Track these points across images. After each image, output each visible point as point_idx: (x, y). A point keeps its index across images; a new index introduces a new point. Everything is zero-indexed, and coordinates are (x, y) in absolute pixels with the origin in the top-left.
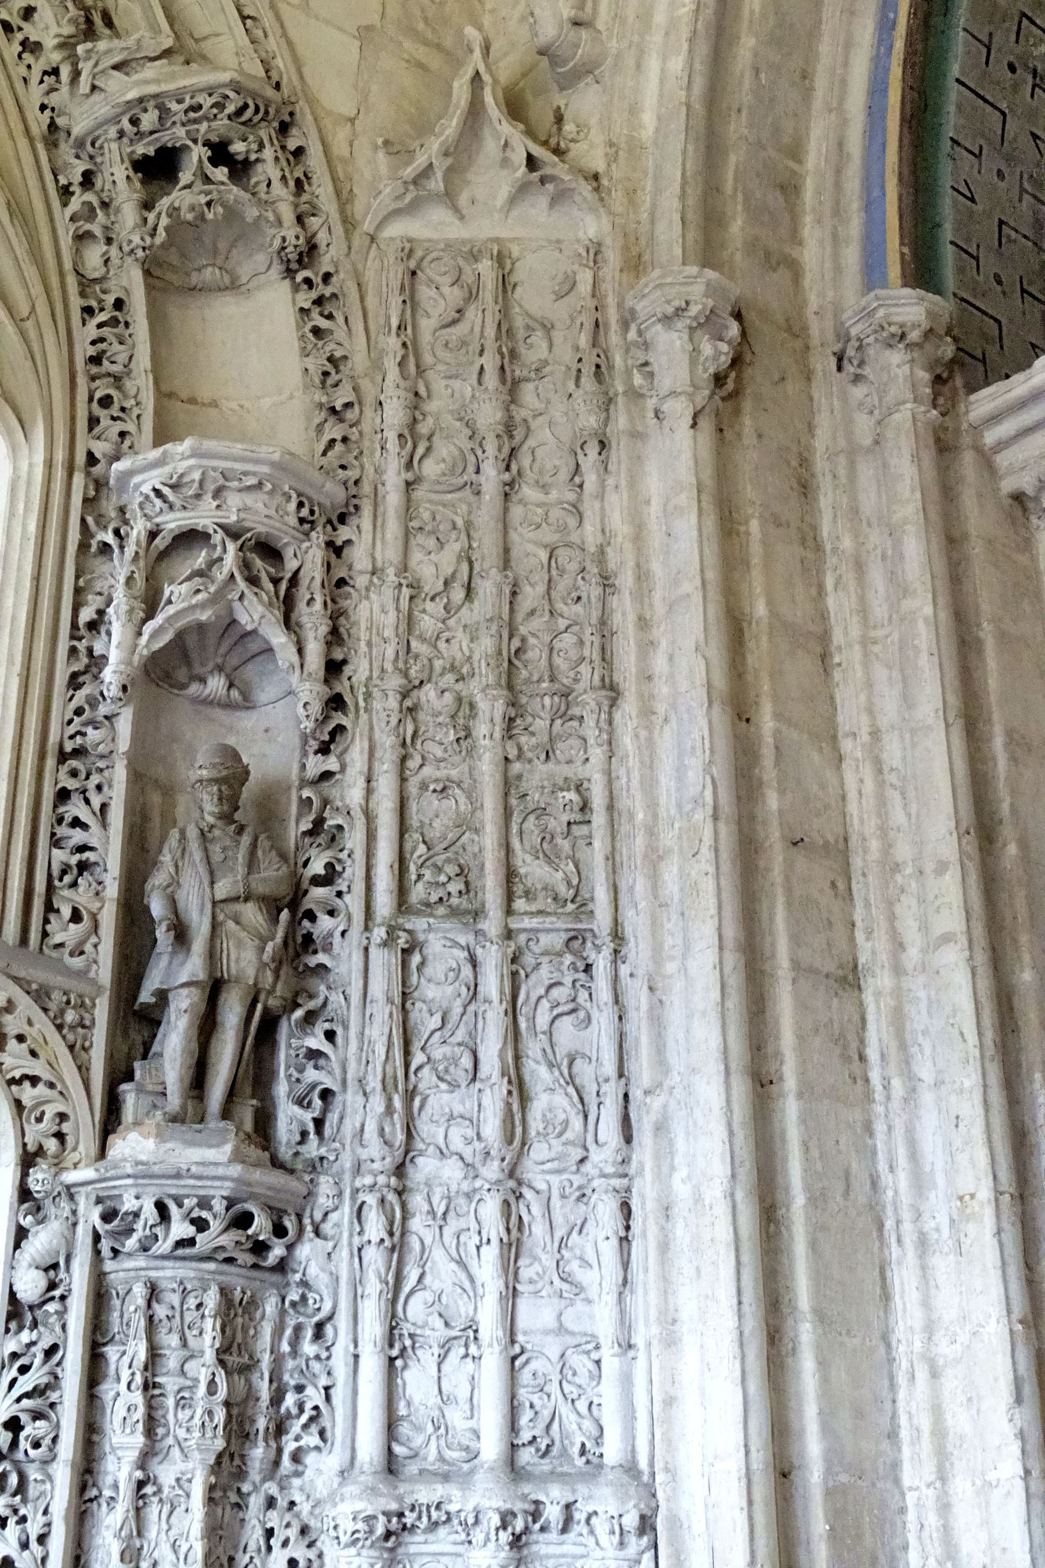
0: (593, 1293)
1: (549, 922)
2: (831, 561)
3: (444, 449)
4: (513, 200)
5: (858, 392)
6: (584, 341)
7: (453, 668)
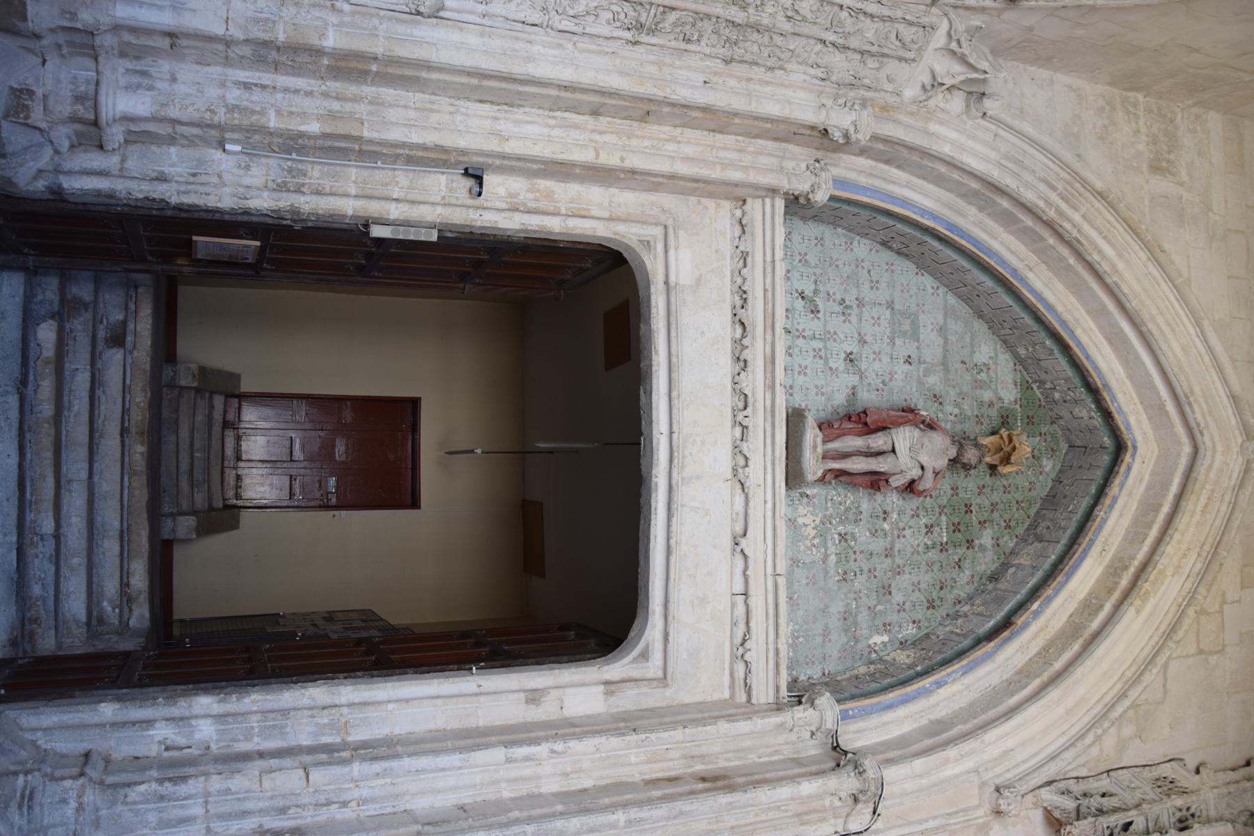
0: (507, 5)
1: (650, 19)
2: (748, 140)
3: (849, 21)
4: (933, 72)
5: (803, 166)
6: (866, 81)
7: (762, 4)
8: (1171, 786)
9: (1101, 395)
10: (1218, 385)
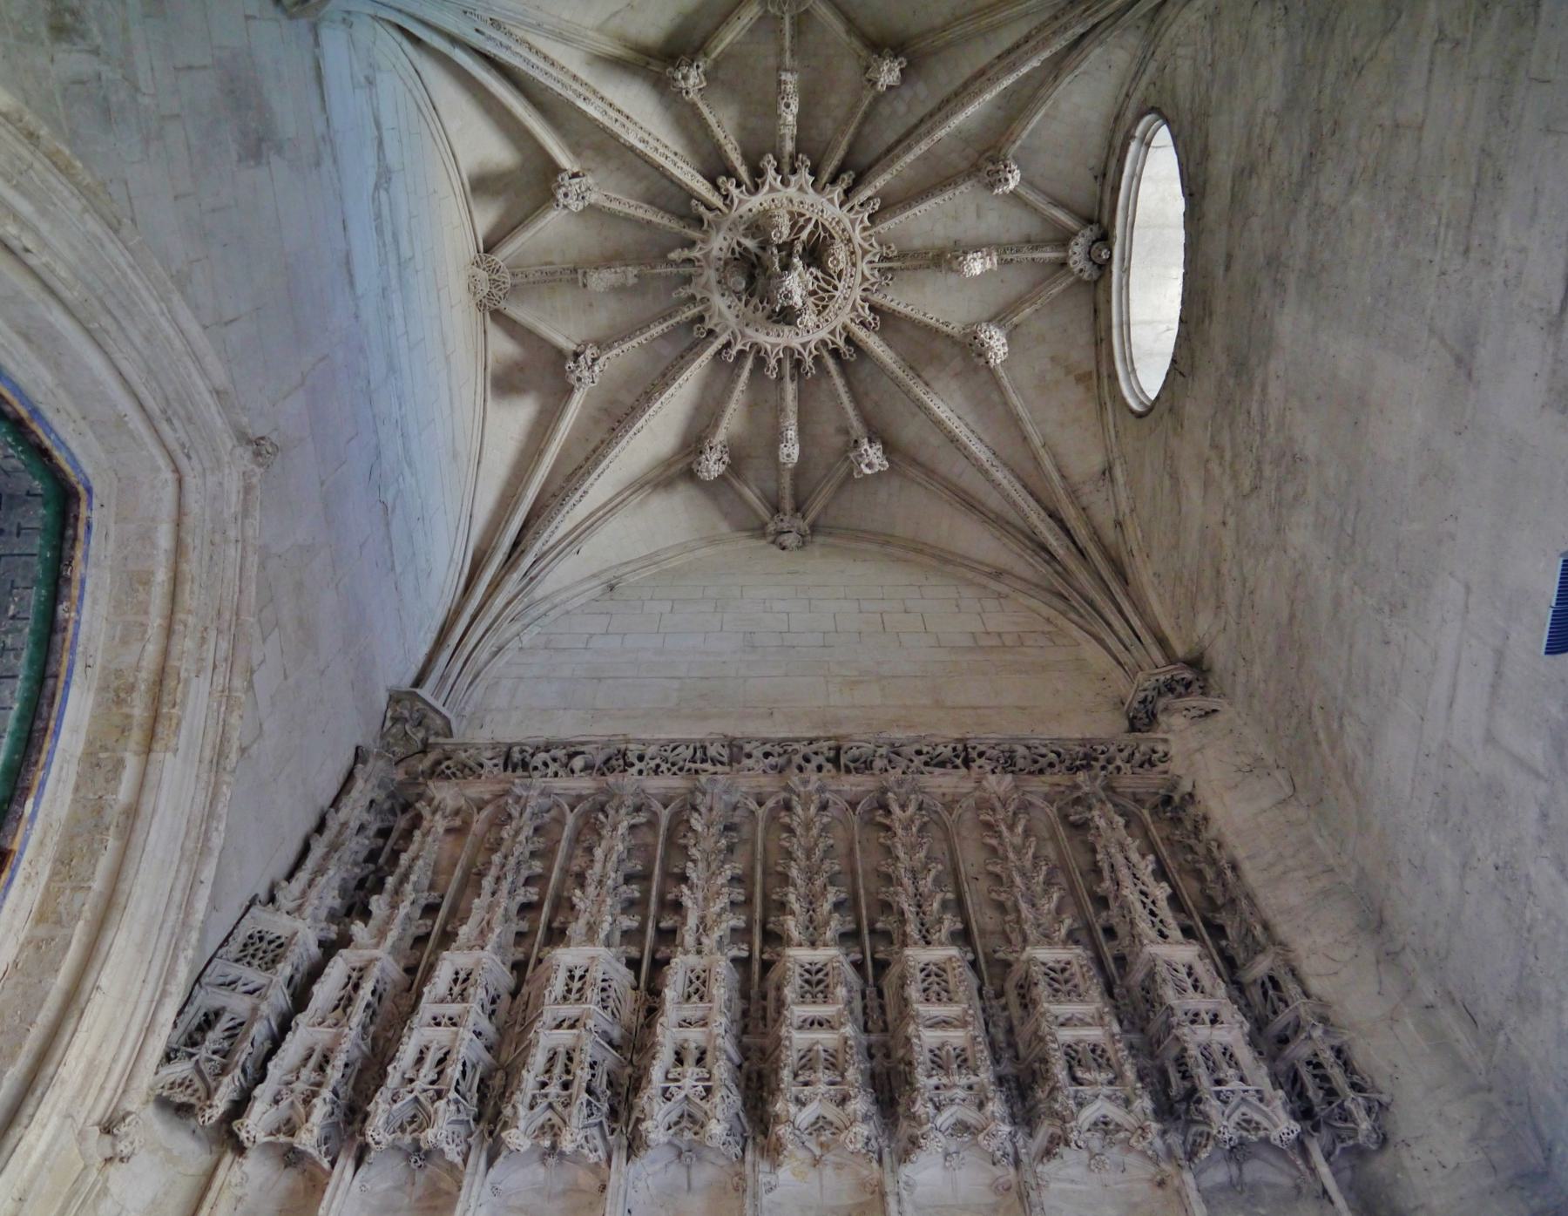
8: (264, 945)
9: (27, 427)
10: (196, 377)
